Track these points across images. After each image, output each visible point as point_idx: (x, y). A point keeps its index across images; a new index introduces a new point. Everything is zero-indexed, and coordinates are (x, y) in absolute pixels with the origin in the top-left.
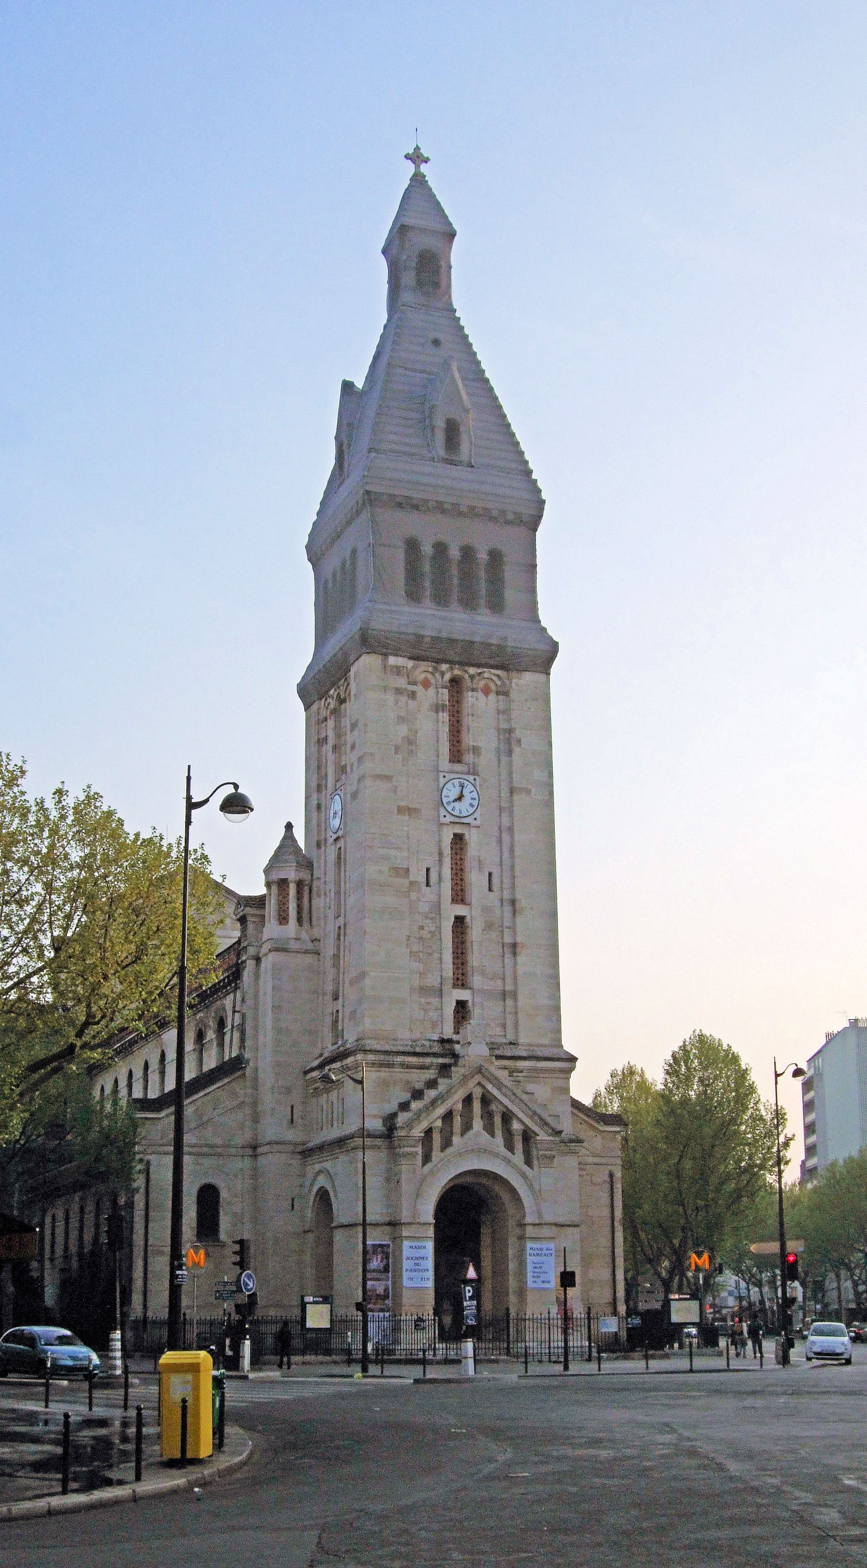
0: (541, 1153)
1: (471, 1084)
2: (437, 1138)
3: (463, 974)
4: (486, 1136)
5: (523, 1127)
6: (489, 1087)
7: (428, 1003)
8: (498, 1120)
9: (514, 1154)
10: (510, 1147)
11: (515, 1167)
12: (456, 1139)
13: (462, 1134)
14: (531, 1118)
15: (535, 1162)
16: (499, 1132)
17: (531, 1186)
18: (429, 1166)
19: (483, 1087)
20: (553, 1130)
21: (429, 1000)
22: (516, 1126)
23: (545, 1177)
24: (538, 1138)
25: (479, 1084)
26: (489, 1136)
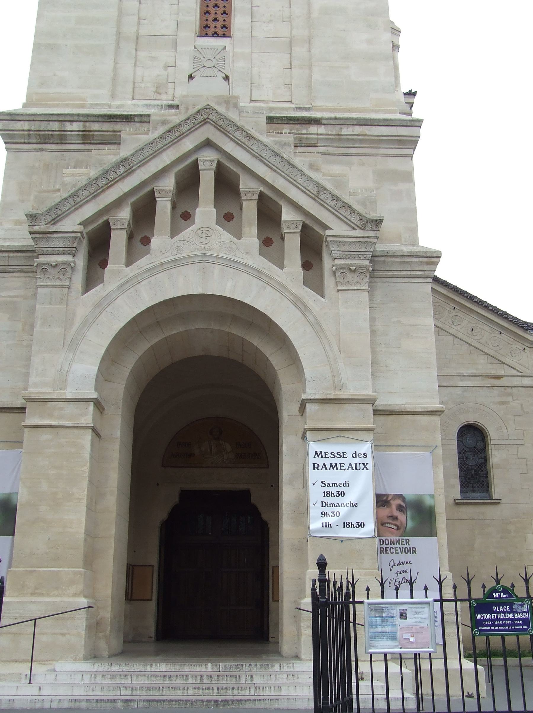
0: (337, 262)
2: (118, 241)
3: (224, 26)
5: (298, 218)
6: (229, 147)
7: (153, 58)
9: (281, 266)
11: (281, 288)
14: (315, 198)
15: (329, 282)
17: (317, 326)
18: (97, 292)
20: (362, 217)
21: (154, 54)
22: (287, 215)
24: (328, 232)
25: (208, 144)
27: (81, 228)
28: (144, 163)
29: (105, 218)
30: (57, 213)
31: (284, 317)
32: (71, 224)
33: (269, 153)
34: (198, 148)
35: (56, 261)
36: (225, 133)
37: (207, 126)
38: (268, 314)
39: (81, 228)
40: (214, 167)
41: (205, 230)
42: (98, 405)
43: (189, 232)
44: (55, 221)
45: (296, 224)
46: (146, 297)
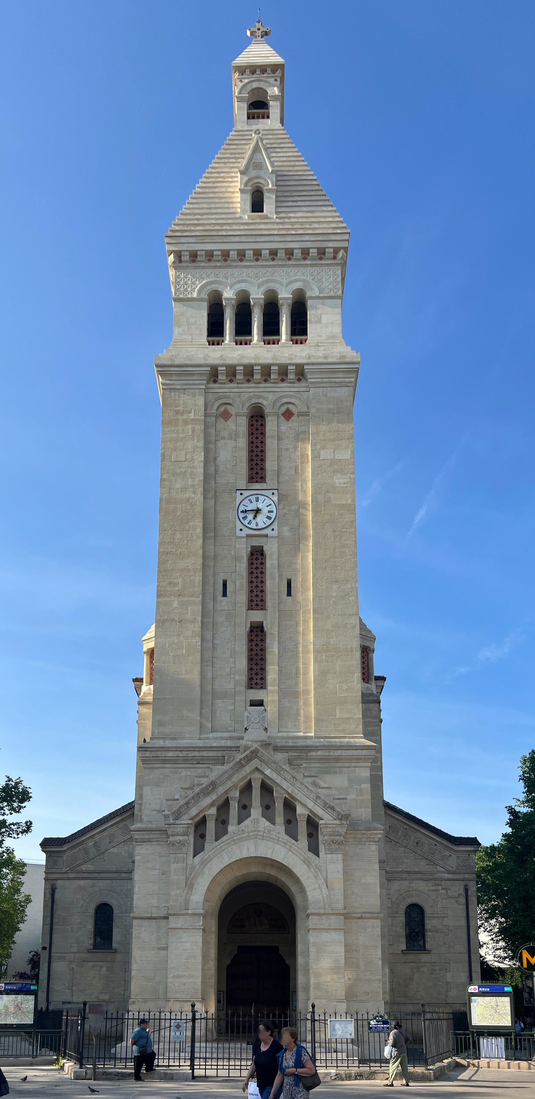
1: (248, 769)
2: (211, 826)
4: (264, 823)
5: (307, 812)
6: (268, 772)
8: (279, 806)
10: (292, 833)
12: (231, 828)
13: (239, 823)
16: (280, 819)
19: (262, 772)
22: (300, 810)
23: (332, 863)
25: (257, 769)
26: (268, 823)
27: (190, 822)
28: (223, 783)
29: (203, 815)
30: (178, 815)
31: (300, 869)
32: (185, 820)
33: (290, 776)
34: (252, 772)
35: (179, 840)
36: (266, 764)
37: (256, 759)
38: (290, 867)
39: (190, 822)
40: (260, 782)
41: (256, 821)
42: (204, 916)
43: (247, 822)
44: (177, 819)
45: (304, 815)
46: (226, 860)
